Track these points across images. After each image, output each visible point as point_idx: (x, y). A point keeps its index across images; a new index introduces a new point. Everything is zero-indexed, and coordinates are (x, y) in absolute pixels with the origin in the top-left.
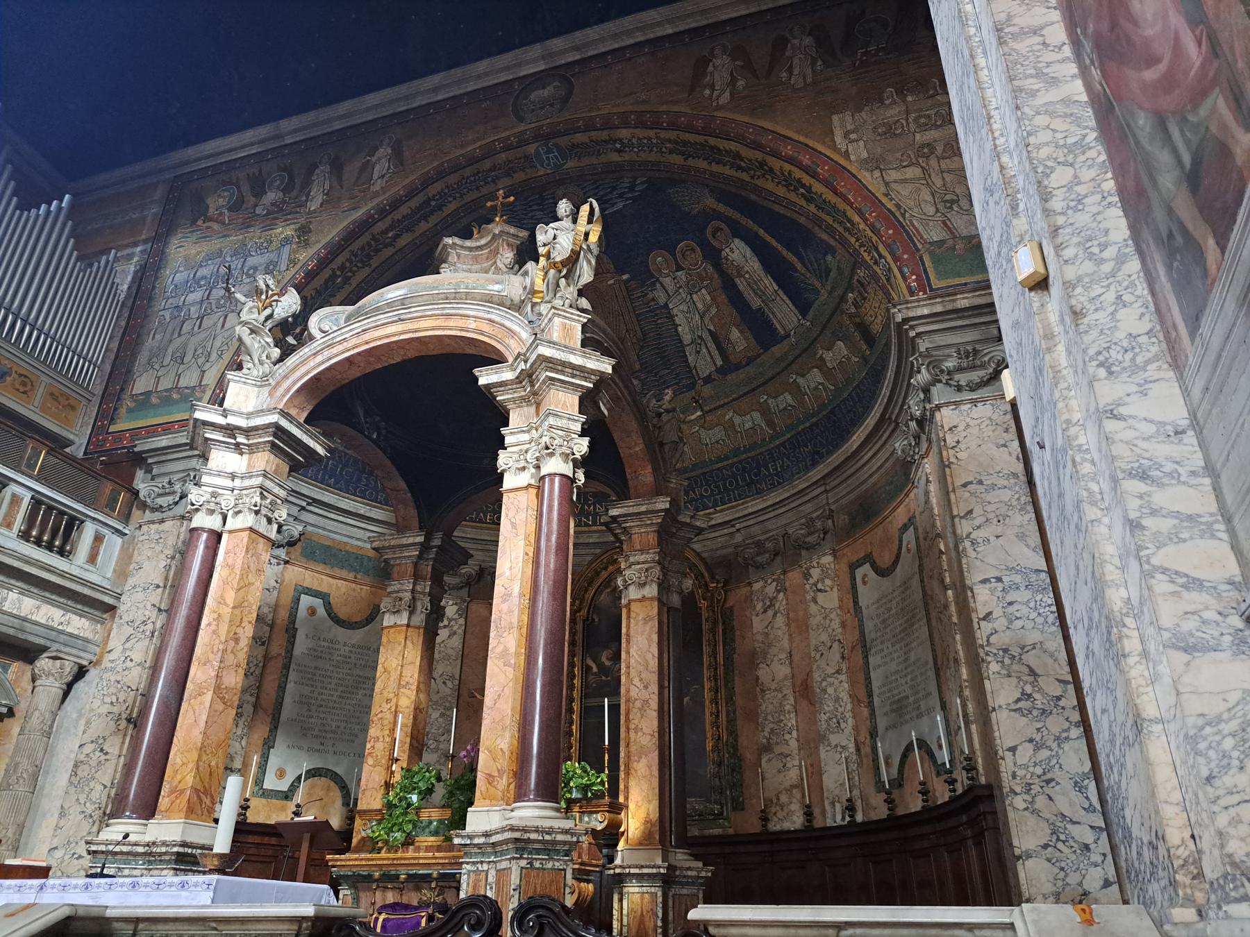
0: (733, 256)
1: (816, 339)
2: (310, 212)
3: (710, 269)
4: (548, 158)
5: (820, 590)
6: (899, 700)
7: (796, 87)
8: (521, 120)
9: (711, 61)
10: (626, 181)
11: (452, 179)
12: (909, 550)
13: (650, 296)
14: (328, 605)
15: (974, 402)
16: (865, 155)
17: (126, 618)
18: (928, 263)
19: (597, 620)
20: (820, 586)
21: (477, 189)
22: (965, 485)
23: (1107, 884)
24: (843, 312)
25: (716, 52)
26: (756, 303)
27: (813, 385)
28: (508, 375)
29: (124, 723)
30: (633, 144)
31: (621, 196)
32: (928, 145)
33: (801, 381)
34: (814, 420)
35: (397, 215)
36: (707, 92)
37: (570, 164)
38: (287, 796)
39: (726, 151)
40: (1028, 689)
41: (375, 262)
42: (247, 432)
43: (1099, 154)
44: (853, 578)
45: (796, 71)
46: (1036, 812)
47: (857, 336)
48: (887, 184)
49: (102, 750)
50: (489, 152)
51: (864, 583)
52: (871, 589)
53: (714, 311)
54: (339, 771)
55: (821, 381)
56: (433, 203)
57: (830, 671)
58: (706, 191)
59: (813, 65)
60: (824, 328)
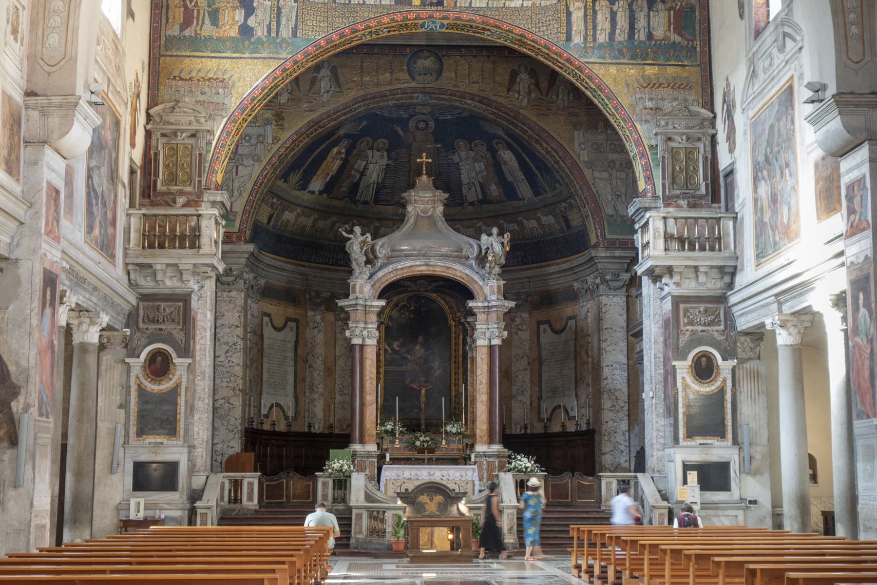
0: (503, 155)
1: (538, 208)
2: (279, 104)
3: (489, 155)
5: (520, 329)
6: (555, 388)
7: (560, 107)
8: (413, 79)
10: (458, 111)
12: (571, 329)
13: (450, 157)
14: (271, 320)
15: (614, 296)
16: (586, 159)
17: (222, 340)
18: (606, 225)
19: (390, 324)
20: (520, 327)
22: (606, 329)
23: (626, 461)
24: (557, 206)
25: (522, 69)
26: (510, 179)
27: (531, 226)
28: (480, 304)
29: (238, 392)
32: (613, 161)
33: (525, 221)
34: (528, 242)
36: (516, 95)
37: (433, 101)
38: (267, 416)
40: (615, 404)
42: (370, 306)
43: (663, 384)
44: (538, 328)
45: (560, 97)
46: (610, 441)
47: (562, 220)
48: (594, 178)
49: (229, 403)
50: (392, 92)
51: (544, 333)
52: (547, 336)
53: (485, 173)
54: (281, 403)
55: (536, 226)
57: (521, 368)
59: (569, 94)
60: (545, 206)
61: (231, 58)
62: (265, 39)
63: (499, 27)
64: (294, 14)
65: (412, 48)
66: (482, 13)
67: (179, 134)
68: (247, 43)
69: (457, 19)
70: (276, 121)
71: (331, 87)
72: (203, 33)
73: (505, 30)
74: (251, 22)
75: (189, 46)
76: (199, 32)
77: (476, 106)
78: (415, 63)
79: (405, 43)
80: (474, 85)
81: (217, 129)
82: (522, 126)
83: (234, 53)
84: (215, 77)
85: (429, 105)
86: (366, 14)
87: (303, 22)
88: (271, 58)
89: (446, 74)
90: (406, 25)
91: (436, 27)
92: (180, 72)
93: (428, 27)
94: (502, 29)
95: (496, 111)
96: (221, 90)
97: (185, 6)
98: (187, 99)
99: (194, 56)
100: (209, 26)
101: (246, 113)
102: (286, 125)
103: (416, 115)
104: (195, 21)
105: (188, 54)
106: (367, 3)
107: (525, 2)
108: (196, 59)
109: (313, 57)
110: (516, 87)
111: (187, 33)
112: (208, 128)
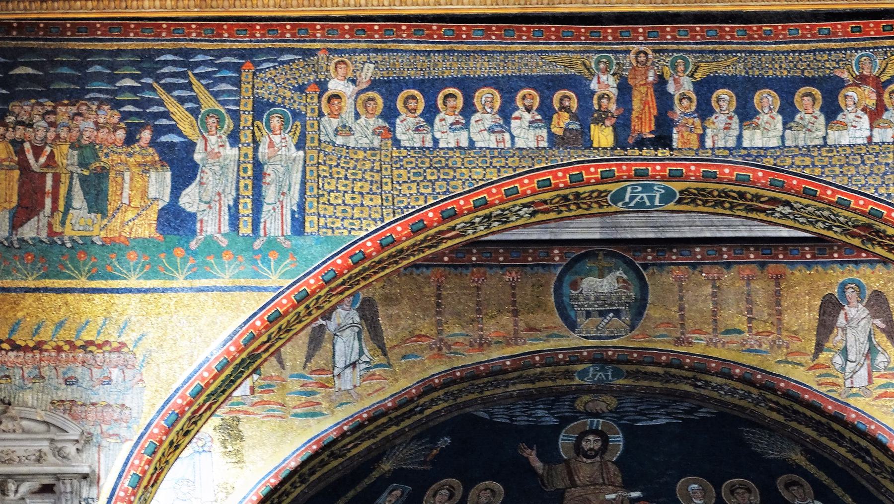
4: (594, 375)
8: (572, 326)
9: (842, 307)
10: (686, 405)
11: (454, 388)
21: (481, 392)
25: (850, 293)
30: (722, 389)
31: (668, 414)
35: (371, 427)
36: (838, 360)
37: (621, 381)
39: (851, 440)
41: (312, 478)
50: (522, 363)
56: (418, 409)
58: (798, 449)
61: (139, 291)
62: (224, 242)
63: (811, 195)
64: (297, 177)
65: (567, 249)
66: (769, 162)
67: (12, 486)
68: (179, 251)
69: (708, 177)
70: (224, 443)
71: (361, 353)
72: (68, 231)
73: (830, 203)
74: (189, 200)
75: (34, 263)
76: (57, 228)
77: (733, 392)
78: (575, 285)
79: (547, 237)
80: (728, 338)
81: (108, 472)
82: (855, 438)
83: (147, 277)
84: (100, 339)
85: (609, 390)
86: (478, 174)
87: (319, 196)
88: (242, 288)
89: (653, 312)
90: (577, 195)
91: (652, 199)
92: (13, 331)
93: (632, 198)
94: (821, 200)
95: (786, 403)
96: (115, 373)
97: (24, 166)
98: (29, 397)
99: (46, 290)
100: (84, 212)
101: (178, 427)
102: (249, 455)
103: (576, 419)
104: (48, 201)
105: (31, 283)
106: (478, 145)
107: (876, 130)
108: (53, 296)
109: (343, 284)
110: (836, 339)
111: (28, 231)
112: (86, 470)
